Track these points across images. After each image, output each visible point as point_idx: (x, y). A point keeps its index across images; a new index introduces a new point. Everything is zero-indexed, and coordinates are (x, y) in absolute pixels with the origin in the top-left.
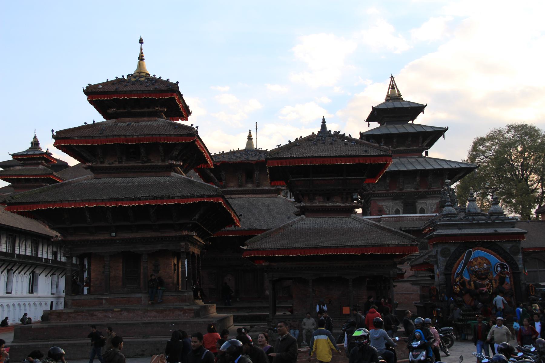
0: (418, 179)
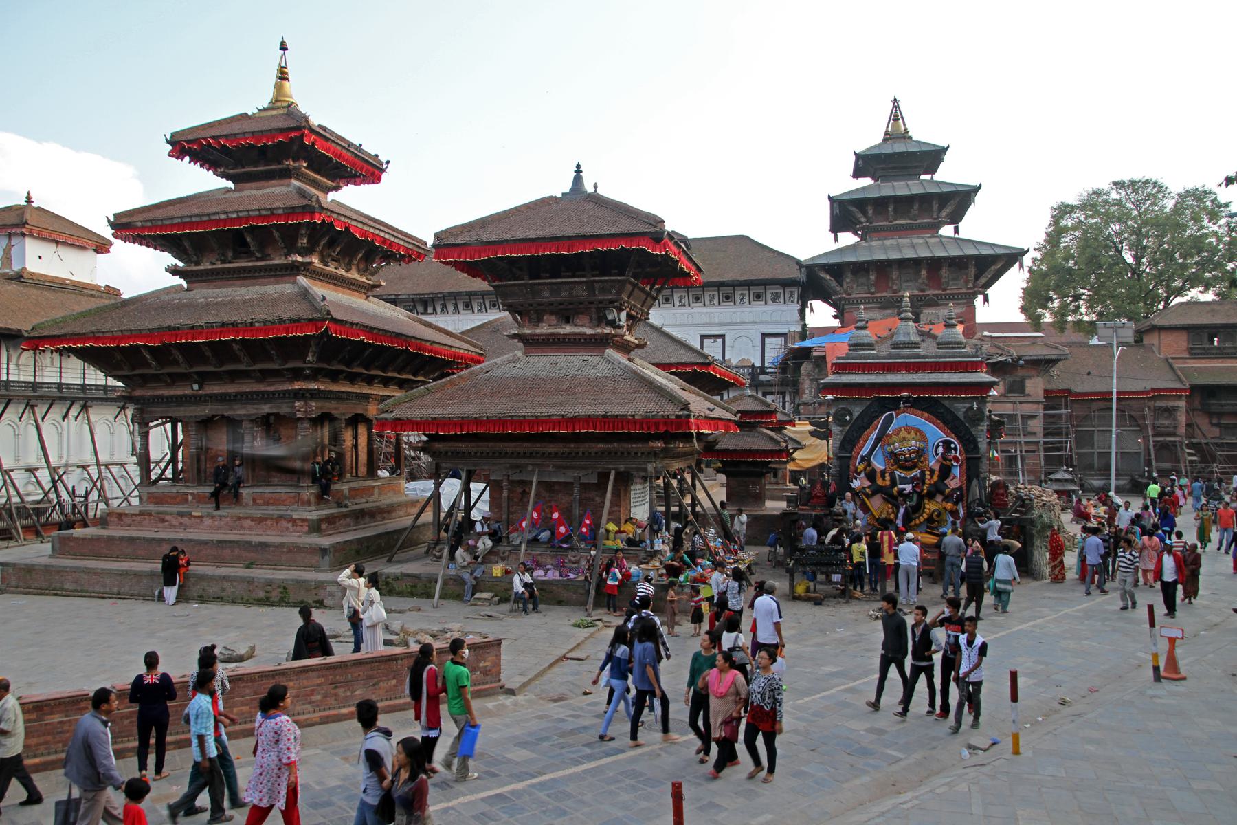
0: (924, 273)
